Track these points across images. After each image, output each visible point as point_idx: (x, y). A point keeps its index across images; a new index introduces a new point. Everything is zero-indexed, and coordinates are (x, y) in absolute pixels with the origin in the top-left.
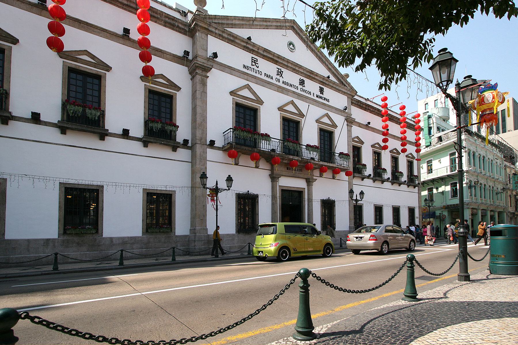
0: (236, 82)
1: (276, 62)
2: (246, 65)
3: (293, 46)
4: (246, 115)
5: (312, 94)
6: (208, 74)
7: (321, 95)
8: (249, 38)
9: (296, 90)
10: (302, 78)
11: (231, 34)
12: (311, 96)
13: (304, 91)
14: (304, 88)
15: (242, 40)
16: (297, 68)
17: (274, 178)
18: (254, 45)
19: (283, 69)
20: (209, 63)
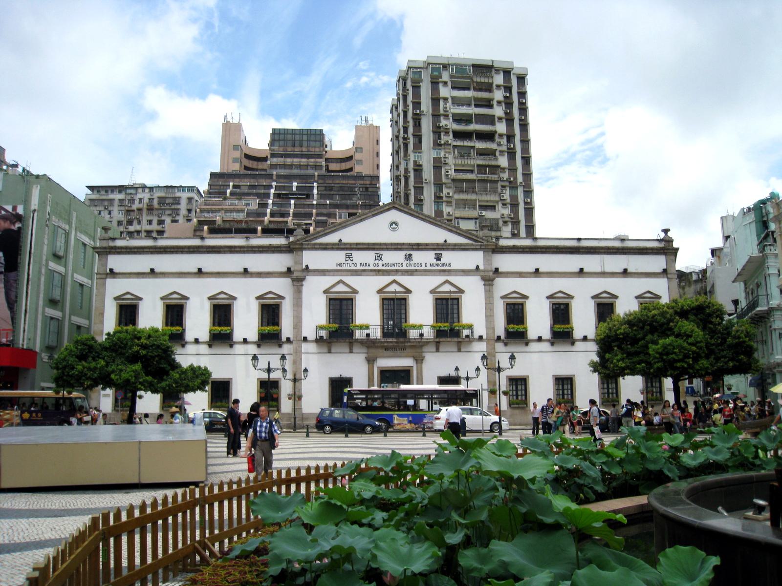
0: (327, 281)
1: (373, 249)
2: (339, 263)
3: (396, 224)
4: (341, 308)
5: (423, 265)
6: (304, 283)
7: (439, 262)
8: (340, 240)
9: (401, 268)
10: (408, 252)
11: (321, 244)
12: (423, 267)
13: (414, 265)
14: (411, 262)
15: (334, 244)
16: (399, 247)
17: (370, 361)
18: (345, 244)
19: (382, 252)
20: (304, 274)
